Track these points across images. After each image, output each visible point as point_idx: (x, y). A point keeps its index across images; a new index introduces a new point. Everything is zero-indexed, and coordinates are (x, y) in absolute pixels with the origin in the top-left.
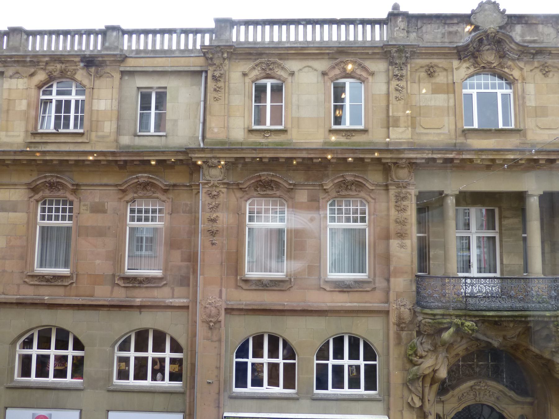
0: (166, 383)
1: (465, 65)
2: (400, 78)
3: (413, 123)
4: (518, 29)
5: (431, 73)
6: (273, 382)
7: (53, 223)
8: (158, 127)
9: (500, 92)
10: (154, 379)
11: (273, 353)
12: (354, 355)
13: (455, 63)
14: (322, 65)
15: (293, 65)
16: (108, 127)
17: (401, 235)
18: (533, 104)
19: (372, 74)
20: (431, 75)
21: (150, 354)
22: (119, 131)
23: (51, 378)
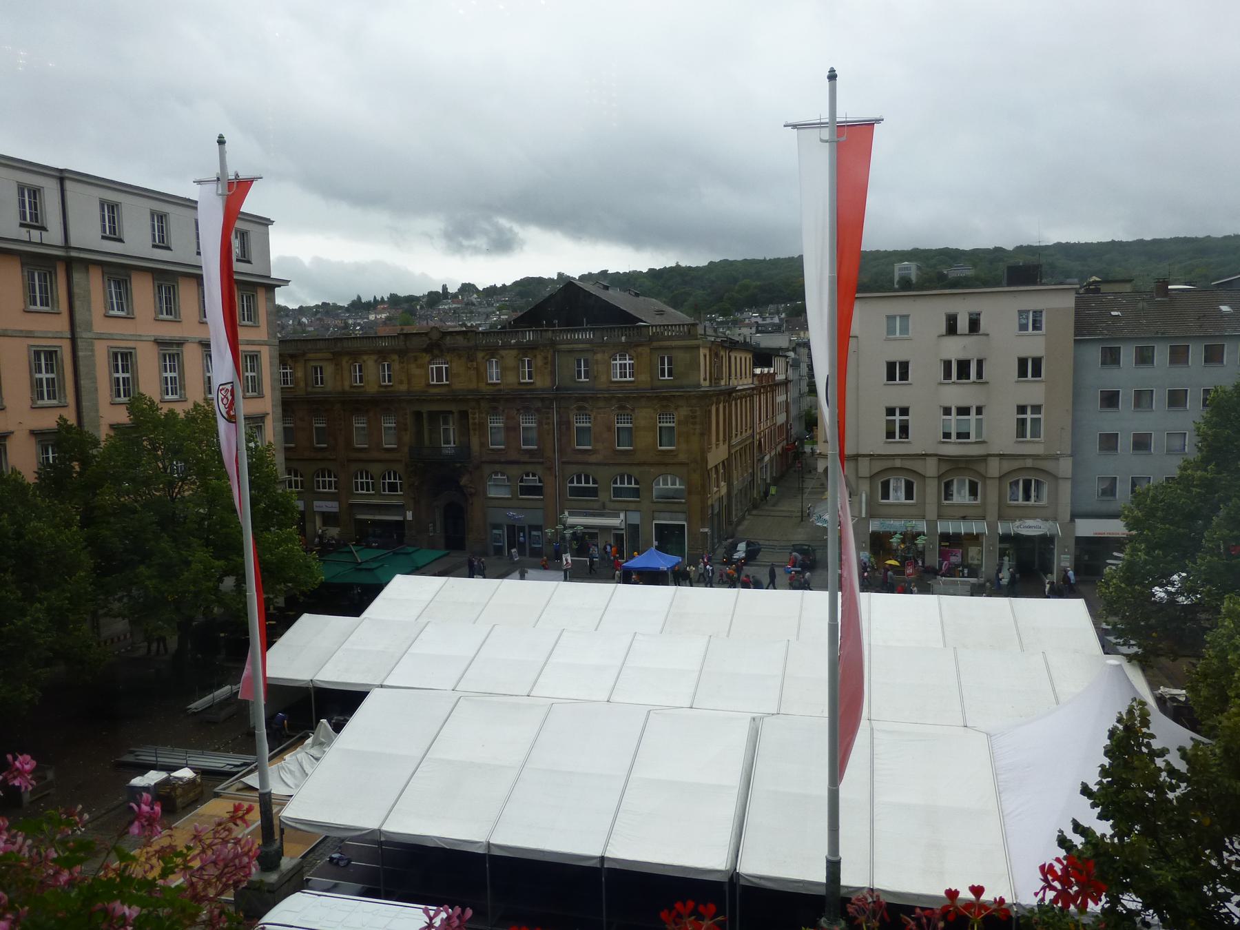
0: (333, 490)
1: (428, 355)
2: (403, 363)
3: (409, 382)
4: (448, 338)
5: (416, 359)
6: (362, 489)
7: (287, 425)
8: (322, 383)
9: (444, 366)
10: (329, 489)
11: (367, 478)
12: (395, 479)
13: (424, 355)
14: (374, 357)
15: (365, 358)
16: (302, 384)
17: (406, 430)
18: (455, 372)
19: (394, 361)
20: (416, 360)
21: (327, 479)
22: (306, 385)
23: (294, 489)
